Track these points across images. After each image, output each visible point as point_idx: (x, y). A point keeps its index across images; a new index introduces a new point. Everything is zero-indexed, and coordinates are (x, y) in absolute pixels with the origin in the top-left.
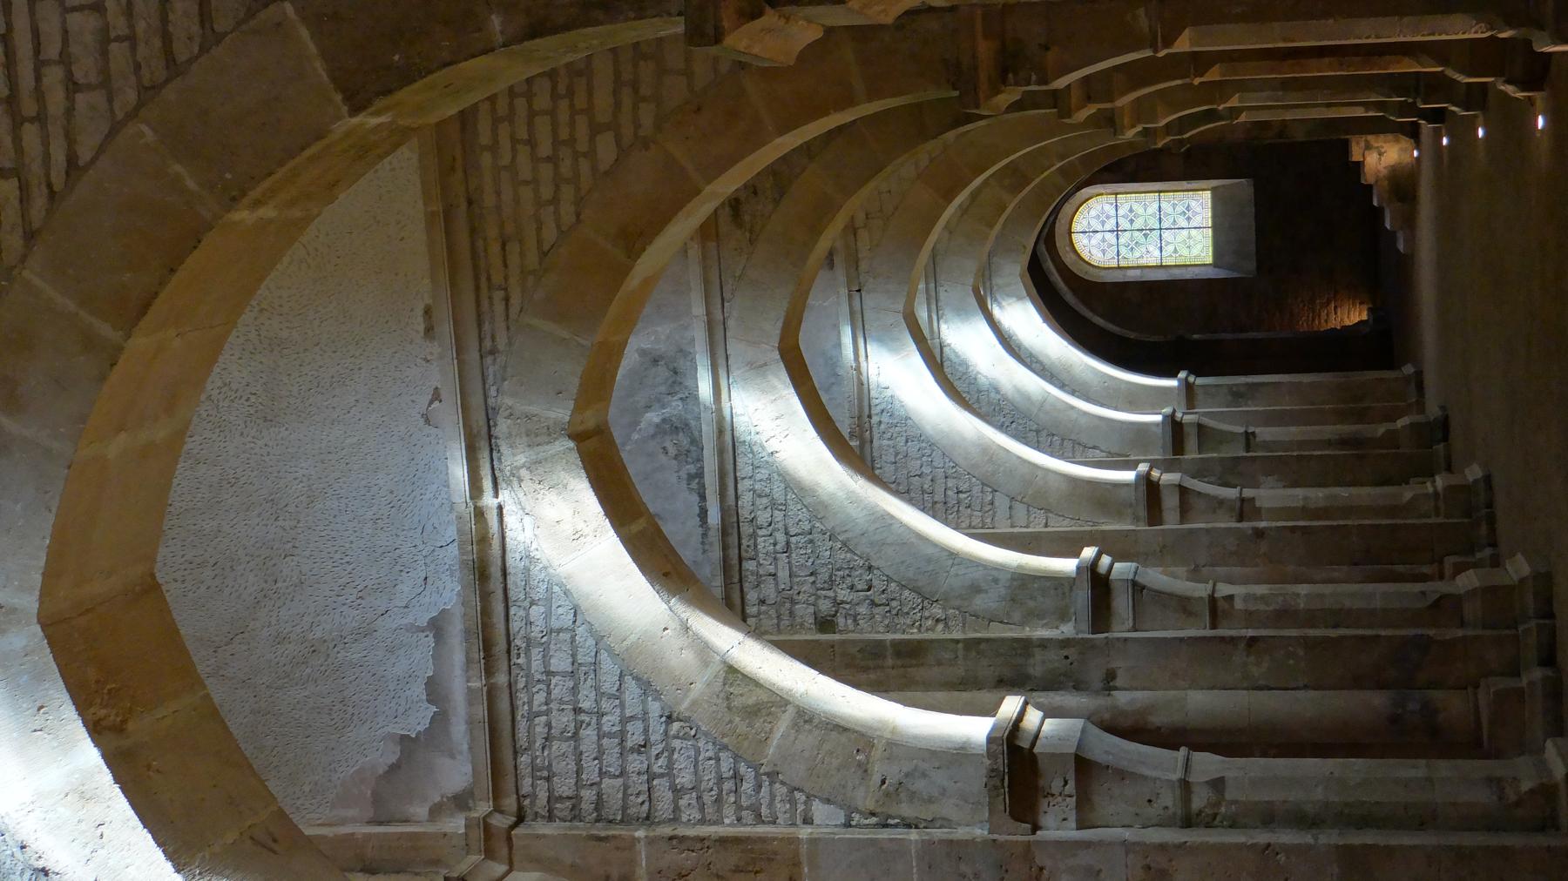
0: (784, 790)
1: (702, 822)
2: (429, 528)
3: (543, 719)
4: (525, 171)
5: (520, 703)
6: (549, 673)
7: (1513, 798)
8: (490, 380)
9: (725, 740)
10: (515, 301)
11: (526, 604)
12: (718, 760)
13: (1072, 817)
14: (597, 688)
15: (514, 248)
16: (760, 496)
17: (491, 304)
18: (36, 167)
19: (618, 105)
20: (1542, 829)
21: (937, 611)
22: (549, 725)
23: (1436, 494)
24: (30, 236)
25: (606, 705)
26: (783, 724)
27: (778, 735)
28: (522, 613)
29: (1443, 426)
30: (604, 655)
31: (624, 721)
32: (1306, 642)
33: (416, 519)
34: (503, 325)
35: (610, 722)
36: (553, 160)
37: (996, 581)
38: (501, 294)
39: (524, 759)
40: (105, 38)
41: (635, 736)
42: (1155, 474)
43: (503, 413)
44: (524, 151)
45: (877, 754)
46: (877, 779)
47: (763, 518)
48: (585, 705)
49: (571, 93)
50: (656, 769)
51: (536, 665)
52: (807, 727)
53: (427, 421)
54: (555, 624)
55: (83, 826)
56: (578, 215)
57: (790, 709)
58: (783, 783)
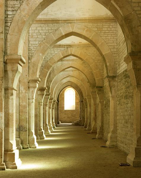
4: (92, 51)
10: (82, 50)
15: (86, 50)
18: (101, 34)
19: (97, 59)
24: (97, 33)
26: (47, 71)
31: (47, 57)
36: (93, 54)
40: (109, 39)
41: (46, 58)
44: (94, 51)
48: (48, 54)
49: (98, 55)
57: (47, 71)
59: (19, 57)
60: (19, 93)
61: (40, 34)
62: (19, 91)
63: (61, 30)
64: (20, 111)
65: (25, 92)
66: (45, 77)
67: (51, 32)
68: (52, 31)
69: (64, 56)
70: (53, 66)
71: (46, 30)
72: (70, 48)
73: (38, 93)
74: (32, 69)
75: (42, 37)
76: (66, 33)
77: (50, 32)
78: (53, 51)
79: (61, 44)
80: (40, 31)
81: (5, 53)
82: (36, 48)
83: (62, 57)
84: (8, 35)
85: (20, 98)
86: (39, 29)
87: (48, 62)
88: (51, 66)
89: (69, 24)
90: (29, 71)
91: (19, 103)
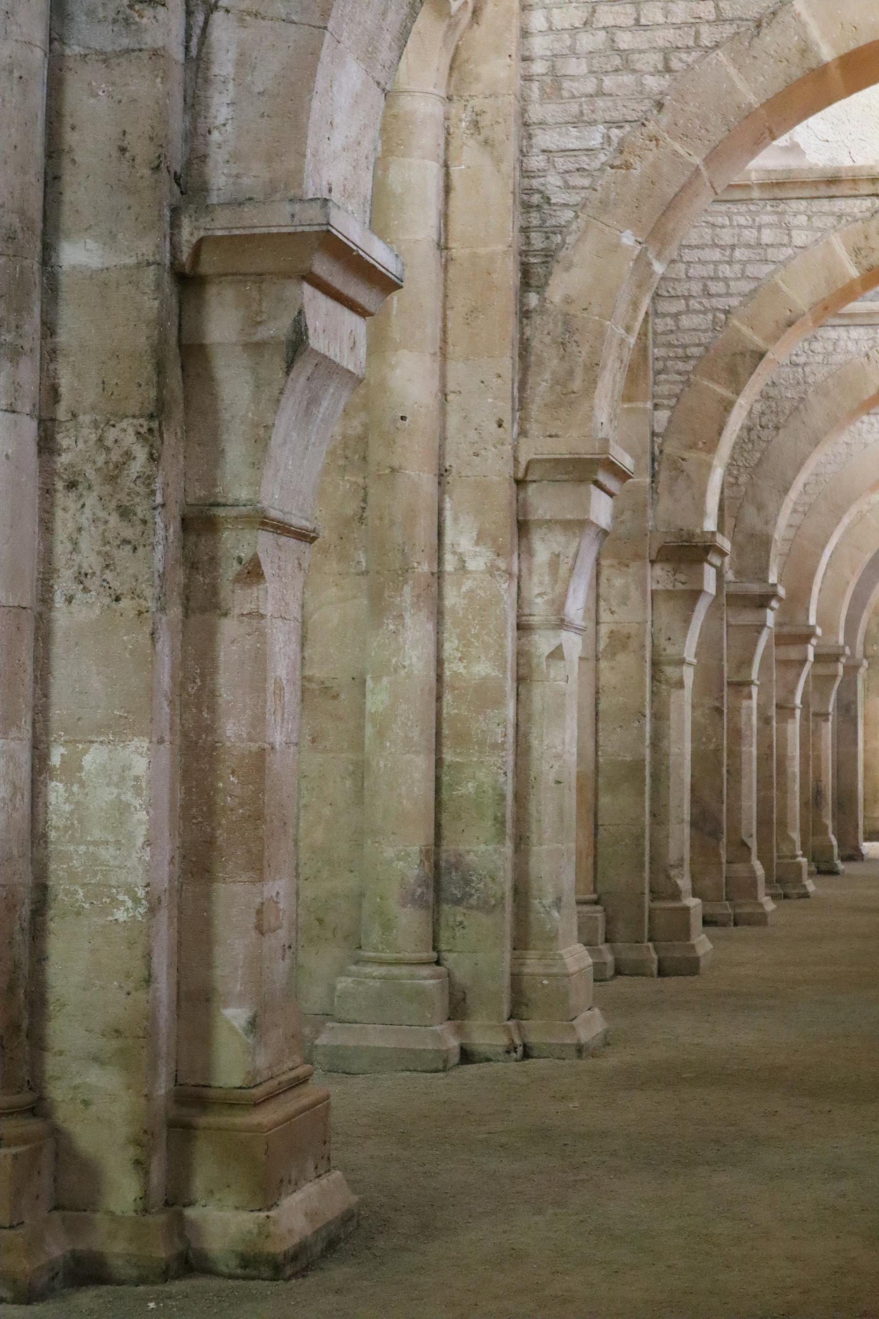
0: (678, 391)
1: (655, 333)
3: (728, 223)
5: (739, 206)
6: (759, 228)
7: (673, 873)
9: (712, 351)
11: (809, 213)
12: (699, 345)
13: (660, 587)
14: (749, 261)
16: (835, 344)
20: (652, 891)
21: (743, 479)
22: (723, 227)
23: (796, 856)
25: (737, 267)
28: (802, 208)
29: (832, 872)
30: (772, 267)
31: (726, 280)
32: (718, 751)
35: (725, 270)
37: (767, 523)
41: (714, 287)
42: (814, 641)
45: (703, 456)
46: (686, 455)
47: (817, 346)
48: (738, 254)
50: (692, 302)
52: (722, 408)
54: (794, 233)
55: (786, 51)
57: (735, 396)
58: (682, 390)
59: (308, 218)
60: (439, 575)
61: (617, 61)
62: (440, 561)
63: (806, 16)
64: (446, 731)
65: (491, 570)
66: (711, 447)
67: (717, 46)
68: (729, 30)
69: (865, 263)
70: (778, 354)
71: (677, 27)
73: (650, 586)
74: (555, 362)
75: (641, 91)
76: (853, 45)
77: (706, 41)
79: (847, 163)
80: (625, 40)
81: (187, 186)
82: (586, 182)
84: (218, 17)
85: (448, 621)
86: (609, 21)
87: (735, 322)
88: (761, 355)
90: (523, 385)
91: (440, 663)
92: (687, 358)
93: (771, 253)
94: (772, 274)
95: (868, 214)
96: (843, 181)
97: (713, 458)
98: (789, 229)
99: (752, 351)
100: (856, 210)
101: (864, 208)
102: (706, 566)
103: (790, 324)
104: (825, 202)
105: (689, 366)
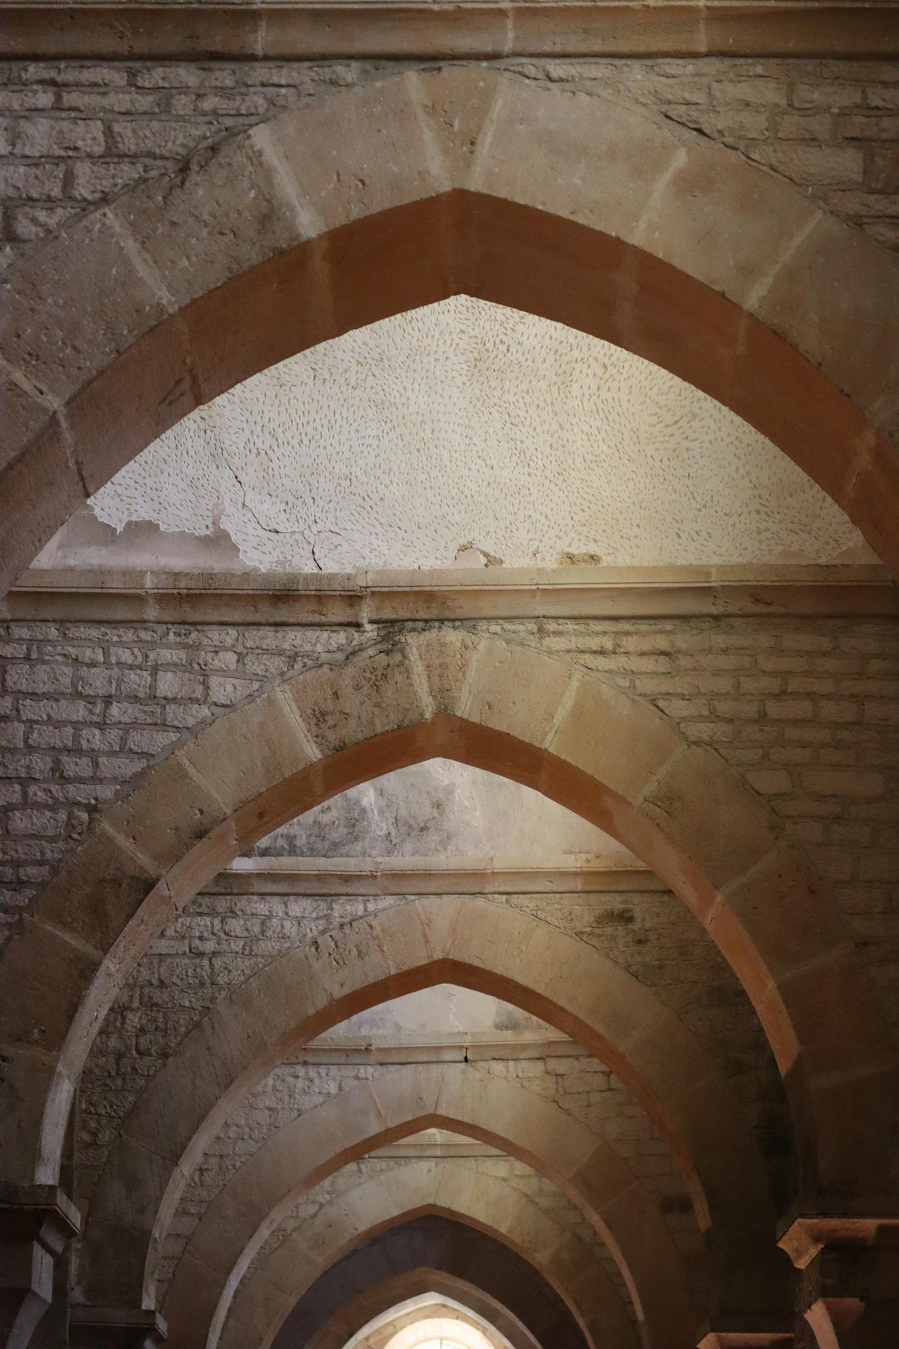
2: (336, 540)
3: (101, 659)
5: (121, 632)
6: (155, 670)
8: (508, 626)
9: (64, 873)
11: (240, 649)
12: (40, 863)
15: (663, 665)
17: (597, 634)
25: (114, 734)
27: (67, 937)
28: (229, 641)
30: (173, 736)
31: (93, 755)
33: (348, 526)
34: (573, 646)
35: (94, 738)
36: (762, 718)
38: (608, 644)
39: (53, 632)
41: (73, 766)
43: (469, 638)
46: (9, 1051)
48: (115, 711)
50: (32, 789)
51: (167, 655)
53: (463, 549)
54: (214, 681)
56: (696, 743)
57: (98, 954)
58: (8, 939)
69: (332, 736)
72: (431, 635)
78: (187, 667)
79: (309, 568)
83: (313, 752)
88: (149, 885)
89: (412, 80)
92: (18, 885)
93: (172, 713)
94: (173, 748)
95: (340, 656)
96: (299, 597)
97: (57, 1060)
98: (205, 675)
99: (132, 878)
100: (319, 648)
101: (334, 646)
102: (38, 1251)
103: (200, 835)
104: (268, 632)
105: (22, 899)
